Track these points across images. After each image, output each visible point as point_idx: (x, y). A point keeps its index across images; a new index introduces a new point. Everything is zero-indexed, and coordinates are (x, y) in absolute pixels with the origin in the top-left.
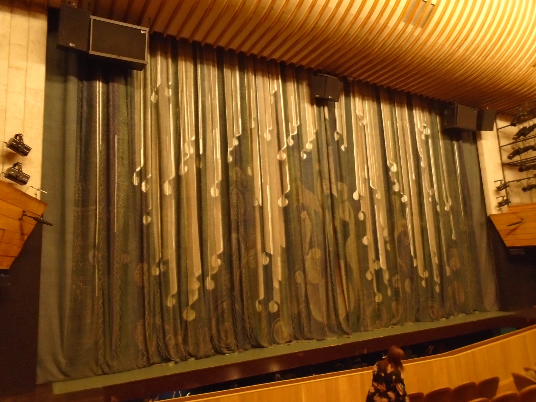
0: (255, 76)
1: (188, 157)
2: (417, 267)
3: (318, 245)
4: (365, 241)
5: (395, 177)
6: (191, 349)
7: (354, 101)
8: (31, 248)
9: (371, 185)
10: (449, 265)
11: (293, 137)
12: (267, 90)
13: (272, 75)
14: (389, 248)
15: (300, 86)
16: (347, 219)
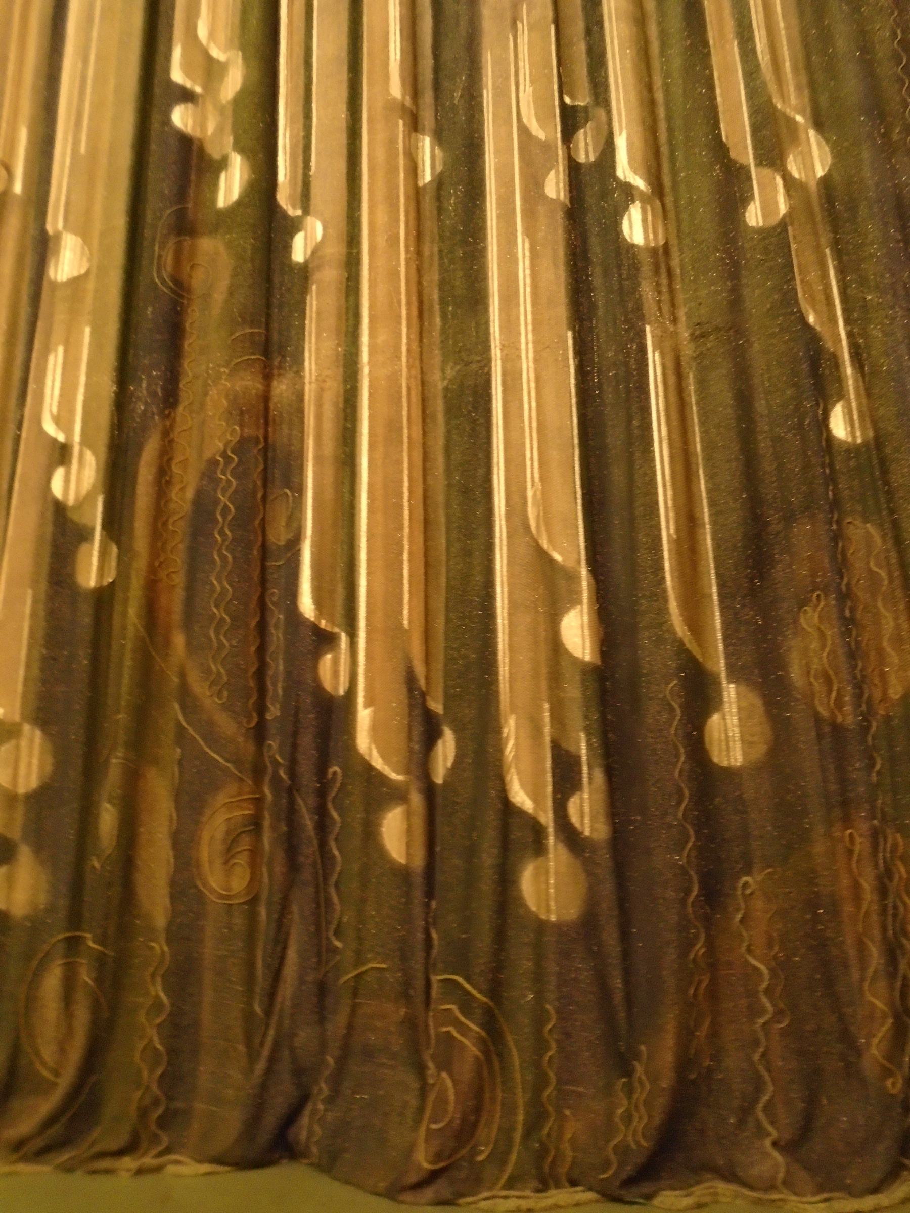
10: (763, 669)
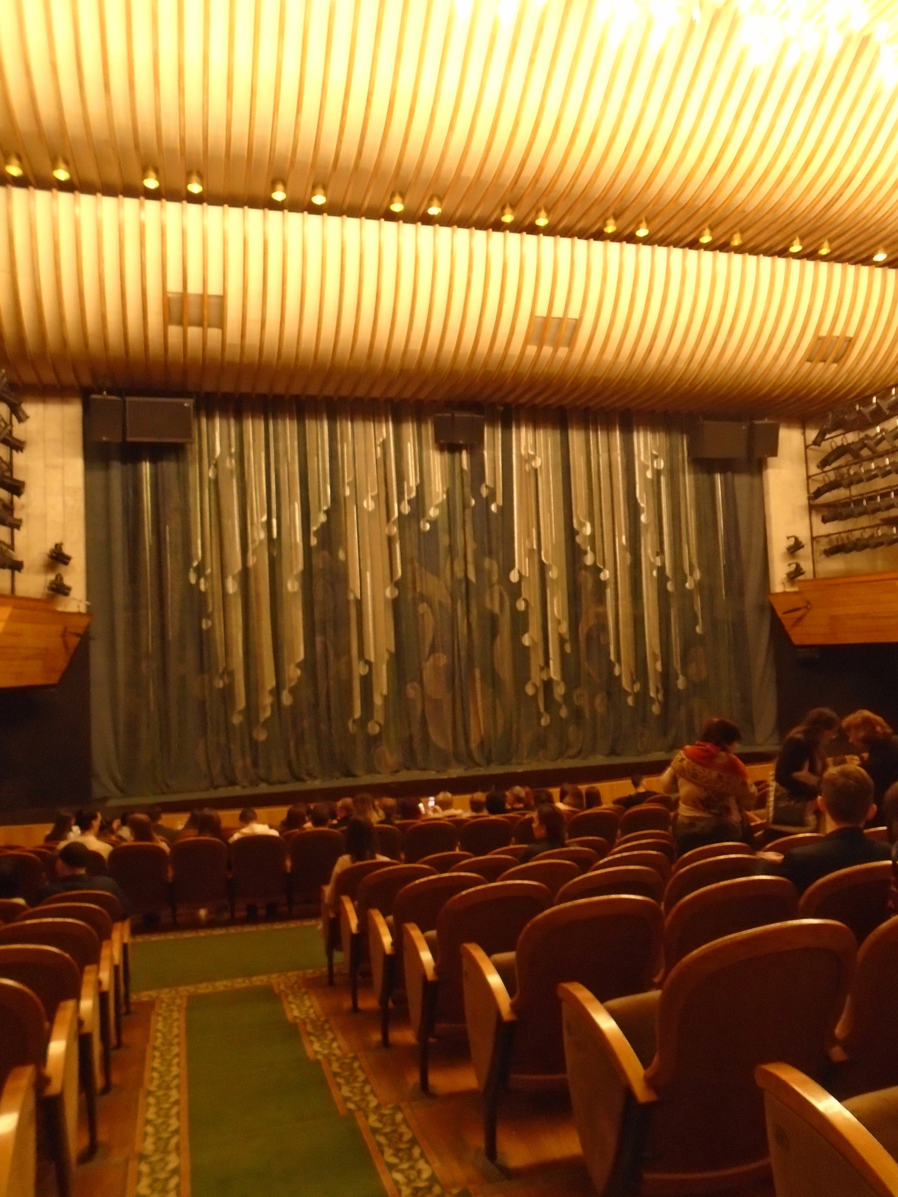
0: (352, 421)
1: (257, 543)
2: (620, 677)
4: (526, 640)
6: (262, 772)
7: (519, 434)
8: (79, 660)
9: (543, 558)
10: (685, 674)
11: (410, 502)
13: (379, 415)
14: (568, 648)
15: (423, 427)
16: (496, 610)
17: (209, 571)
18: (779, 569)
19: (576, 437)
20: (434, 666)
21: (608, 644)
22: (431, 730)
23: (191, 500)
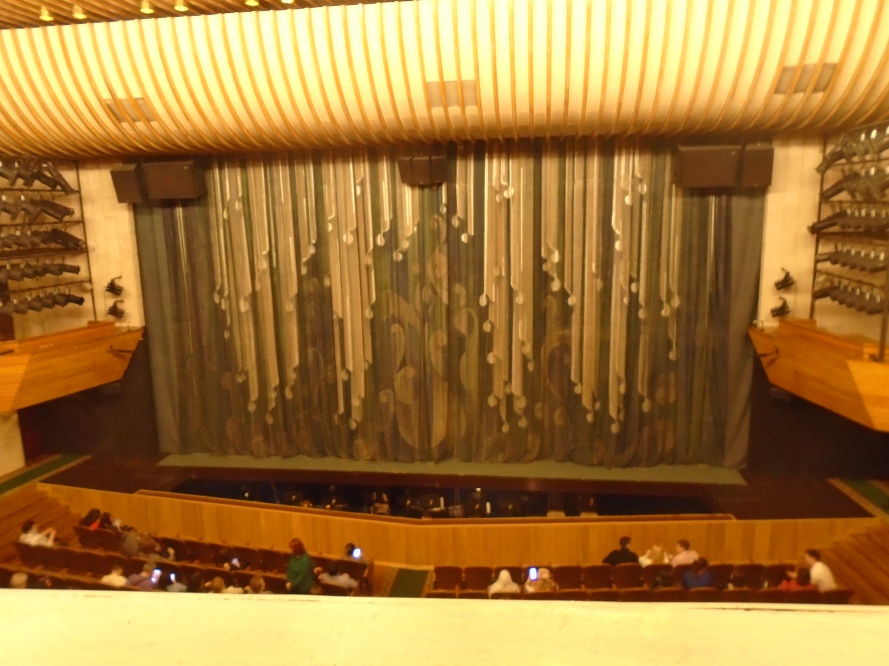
3: (412, 362)
5: (555, 271)
9: (512, 284)
10: (651, 395)
11: (385, 235)
12: (348, 181)
13: (358, 156)
14: (531, 367)
17: (226, 293)
18: (768, 300)
19: (550, 166)
20: (403, 379)
21: (570, 365)
22: (402, 429)
23: (212, 236)
